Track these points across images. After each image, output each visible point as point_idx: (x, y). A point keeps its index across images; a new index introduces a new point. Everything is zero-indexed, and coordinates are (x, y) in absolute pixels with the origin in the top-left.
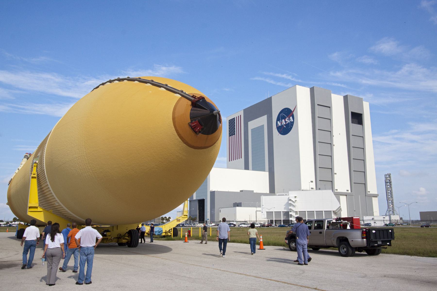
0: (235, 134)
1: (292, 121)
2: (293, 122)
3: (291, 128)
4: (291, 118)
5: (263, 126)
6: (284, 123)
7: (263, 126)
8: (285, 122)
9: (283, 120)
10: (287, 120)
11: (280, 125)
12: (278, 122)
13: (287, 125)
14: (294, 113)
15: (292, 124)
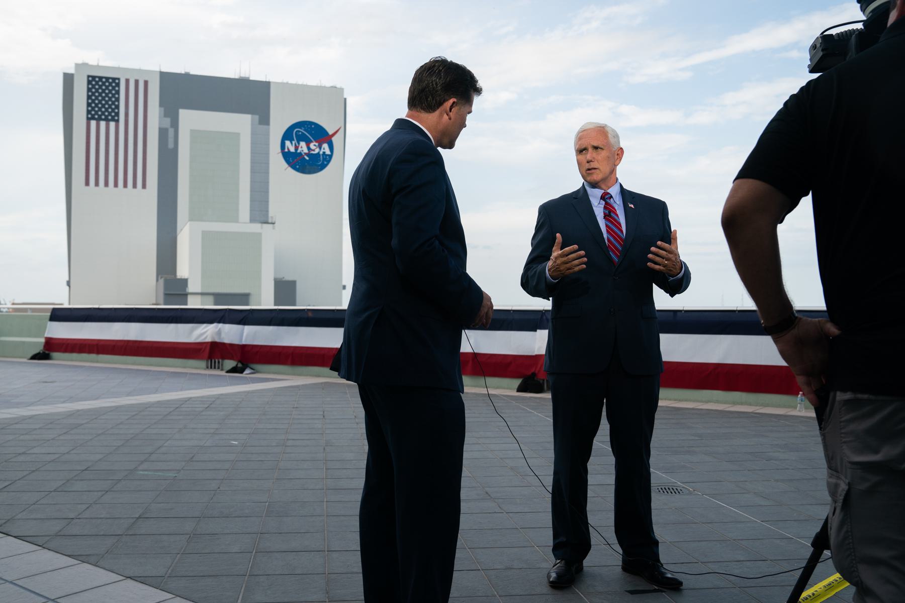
0: (117, 121)
1: (328, 152)
2: (331, 156)
3: (323, 167)
4: (325, 146)
5: (236, 136)
6: (306, 151)
7: (236, 136)
8: (309, 148)
9: (303, 144)
10: (312, 146)
11: (292, 149)
12: (288, 143)
13: (314, 158)
14: (334, 139)
15: (327, 159)
